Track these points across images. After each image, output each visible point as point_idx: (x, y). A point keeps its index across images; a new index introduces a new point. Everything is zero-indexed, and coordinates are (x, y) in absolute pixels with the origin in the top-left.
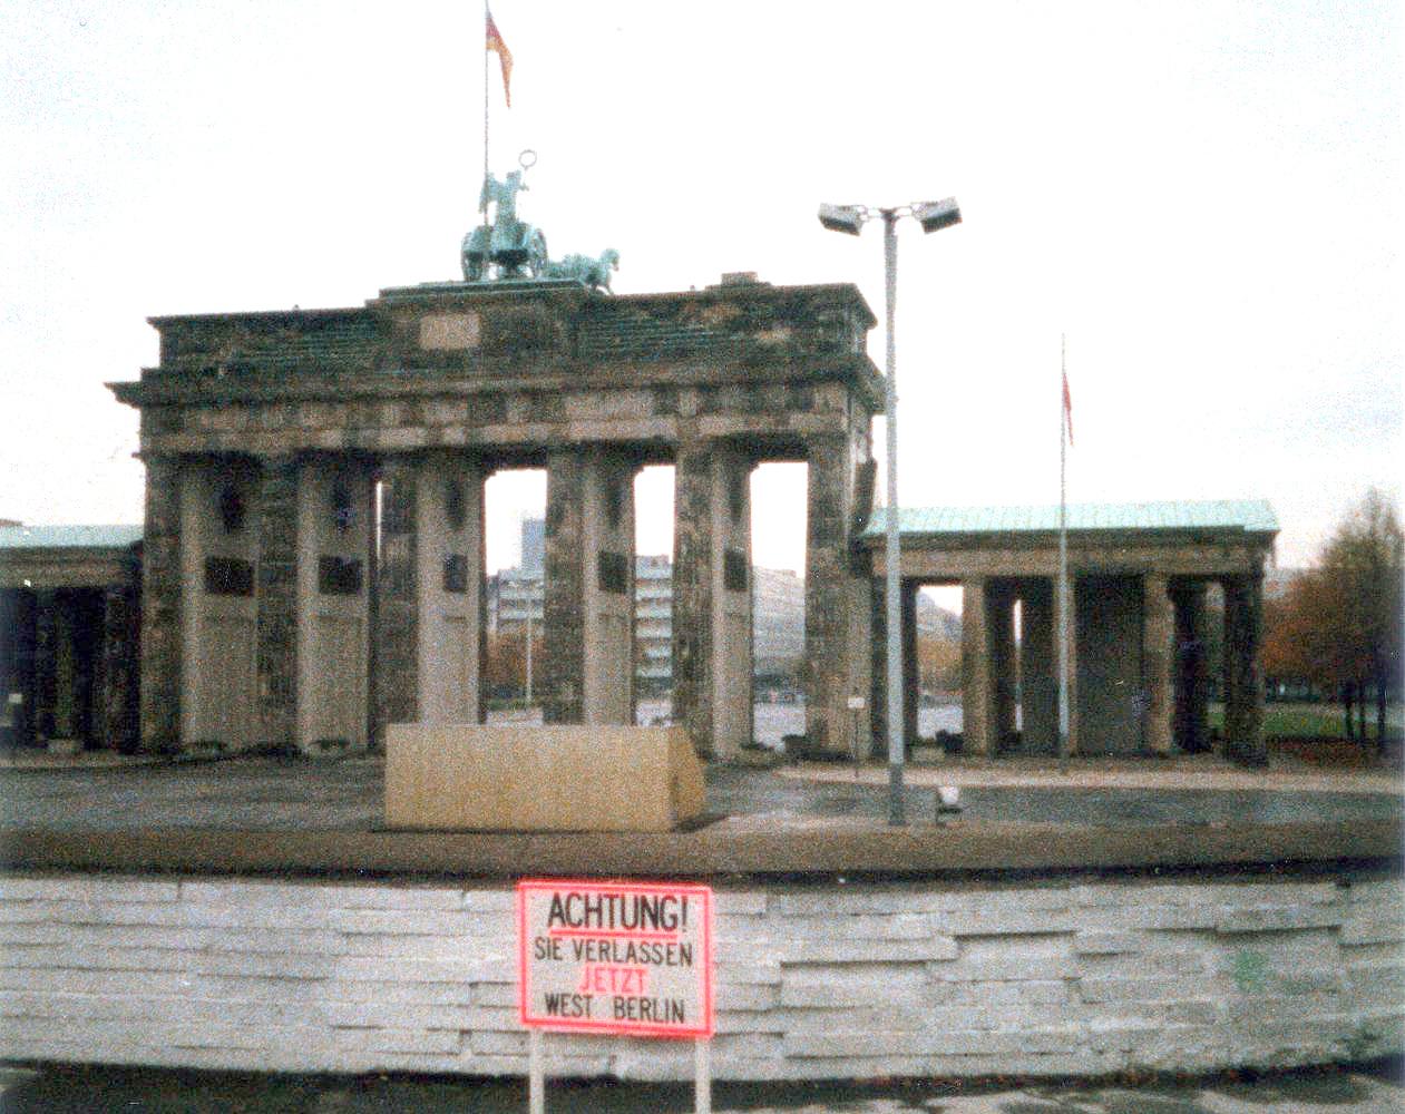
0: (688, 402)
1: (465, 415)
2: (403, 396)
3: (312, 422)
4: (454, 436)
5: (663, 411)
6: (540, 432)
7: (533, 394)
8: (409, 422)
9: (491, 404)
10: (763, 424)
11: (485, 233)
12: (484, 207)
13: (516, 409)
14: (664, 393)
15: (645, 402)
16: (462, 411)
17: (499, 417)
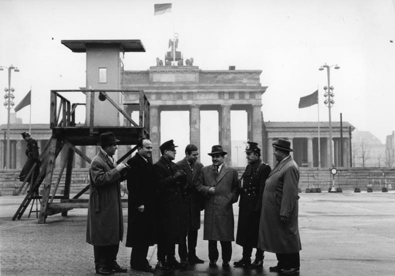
0: (226, 96)
1: (172, 98)
2: (156, 93)
3: (131, 99)
4: (170, 103)
5: (220, 98)
6: (190, 102)
7: (188, 93)
8: (158, 98)
9: (180, 95)
10: (245, 102)
11: (169, 54)
12: (169, 47)
13: (185, 97)
14: (221, 94)
15: (216, 96)
16: (172, 96)
17: (181, 98)
